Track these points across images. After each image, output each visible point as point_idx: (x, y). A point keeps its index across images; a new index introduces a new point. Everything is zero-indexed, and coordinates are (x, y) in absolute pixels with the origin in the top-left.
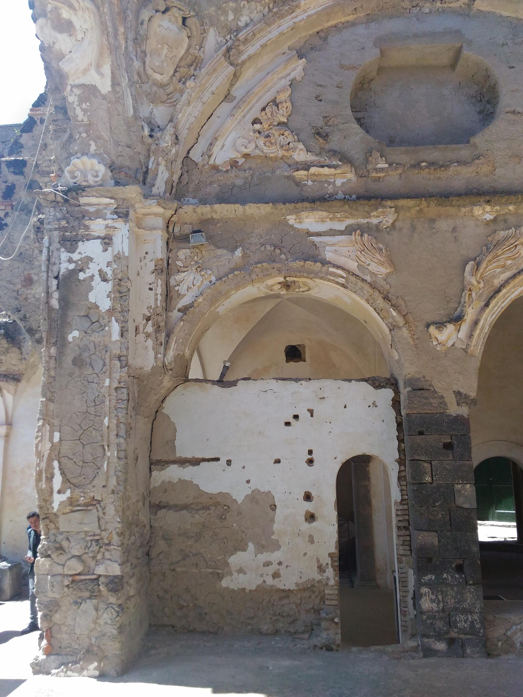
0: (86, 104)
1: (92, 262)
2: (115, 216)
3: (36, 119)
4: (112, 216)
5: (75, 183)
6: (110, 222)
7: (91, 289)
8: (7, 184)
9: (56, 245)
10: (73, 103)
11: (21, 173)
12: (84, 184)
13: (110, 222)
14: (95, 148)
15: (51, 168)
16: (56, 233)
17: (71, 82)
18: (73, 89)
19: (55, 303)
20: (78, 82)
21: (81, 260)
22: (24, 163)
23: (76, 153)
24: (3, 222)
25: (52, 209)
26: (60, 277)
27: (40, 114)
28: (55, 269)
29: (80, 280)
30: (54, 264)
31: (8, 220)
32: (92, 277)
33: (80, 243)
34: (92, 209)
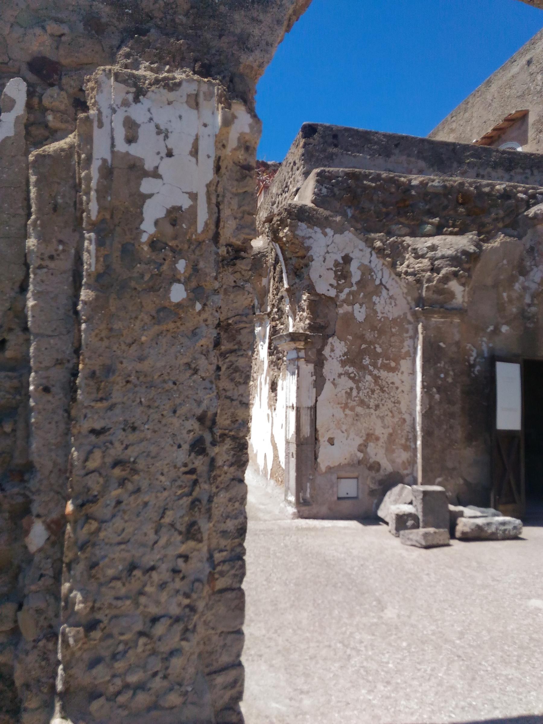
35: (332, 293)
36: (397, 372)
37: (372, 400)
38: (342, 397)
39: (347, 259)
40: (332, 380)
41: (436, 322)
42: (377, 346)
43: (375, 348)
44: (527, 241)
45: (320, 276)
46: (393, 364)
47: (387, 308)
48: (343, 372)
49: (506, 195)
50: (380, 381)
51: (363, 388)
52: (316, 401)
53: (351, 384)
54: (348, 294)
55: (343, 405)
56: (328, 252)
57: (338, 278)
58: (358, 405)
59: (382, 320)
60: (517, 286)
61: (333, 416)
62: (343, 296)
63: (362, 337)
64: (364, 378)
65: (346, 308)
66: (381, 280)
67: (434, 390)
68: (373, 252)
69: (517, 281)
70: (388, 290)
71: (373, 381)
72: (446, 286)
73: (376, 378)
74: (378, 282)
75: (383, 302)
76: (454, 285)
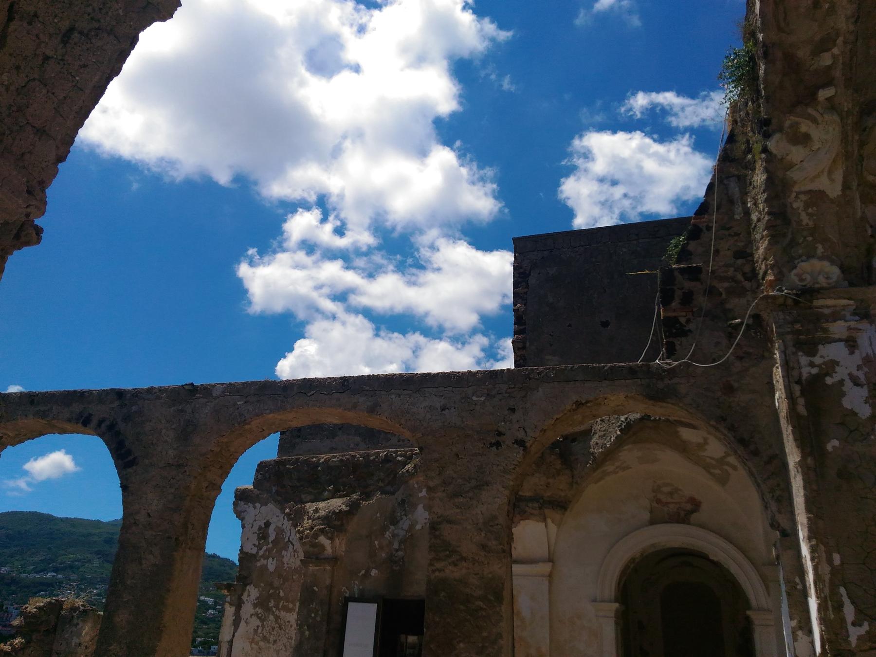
0: (812, 208)
1: (838, 365)
2: (857, 318)
3: (701, 226)
4: (852, 317)
5: (805, 286)
6: (853, 324)
7: (843, 394)
8: (683, 291)
9: (791, 349)
10: (798, 208)
11: (697, 279)
12: (817, 286)
13: (853, 324)
14: (822, 250)
15: (729, 273)
16: (789, 337)
17: (796, 188)
18: (800, 196)
19: (802, 409)
20: (803, 189)
21: (824, 363)
22: (698, 270)
23: (800, 256)
24: (687, 329)
25: (780, 313)
26: (804, 382)
27: (705, 222)
28: (795, 373)
29: (828, 385)
30: (793, 368)
31: (691, 326)
32: (841, 382)
33: (820, 347)
34: (827, 311)
35: (254, 551)
36: (293, 612)
37: (272, 636)
38: (251, 633)
39: (267, 524)
40: (245, 619)
41: (312, 569)
42: (281, 591)
43: (279, 592)
44: (399, 496)
45: (248, 539)
46: (291, 606)
47: (291, 560)
48: (254, 613)
49: (388, 459)
50: (279, 620)
51: (266, 626)
52: (234, 636)
53: (258, 623)
54: (265, 551)
55: (251, 640)
56: (255, 520)
57: (259, 539)
58: (261, 640)
59: (287, 569)
60: (388, 534)
61: (243, 649)
62: (261, 553)
63: (271, 585)
64: (269, 618)
65: (263, 562)
66: (289, 537)
67: (306, 627)
68: (285, 517)
69: (388, 530)
70: (293, 545)
71: (274, 620)
72: (317, 541)
73: (277, 618)
74: (286, 540)
75: (289, 555)
76: (322, 539)
